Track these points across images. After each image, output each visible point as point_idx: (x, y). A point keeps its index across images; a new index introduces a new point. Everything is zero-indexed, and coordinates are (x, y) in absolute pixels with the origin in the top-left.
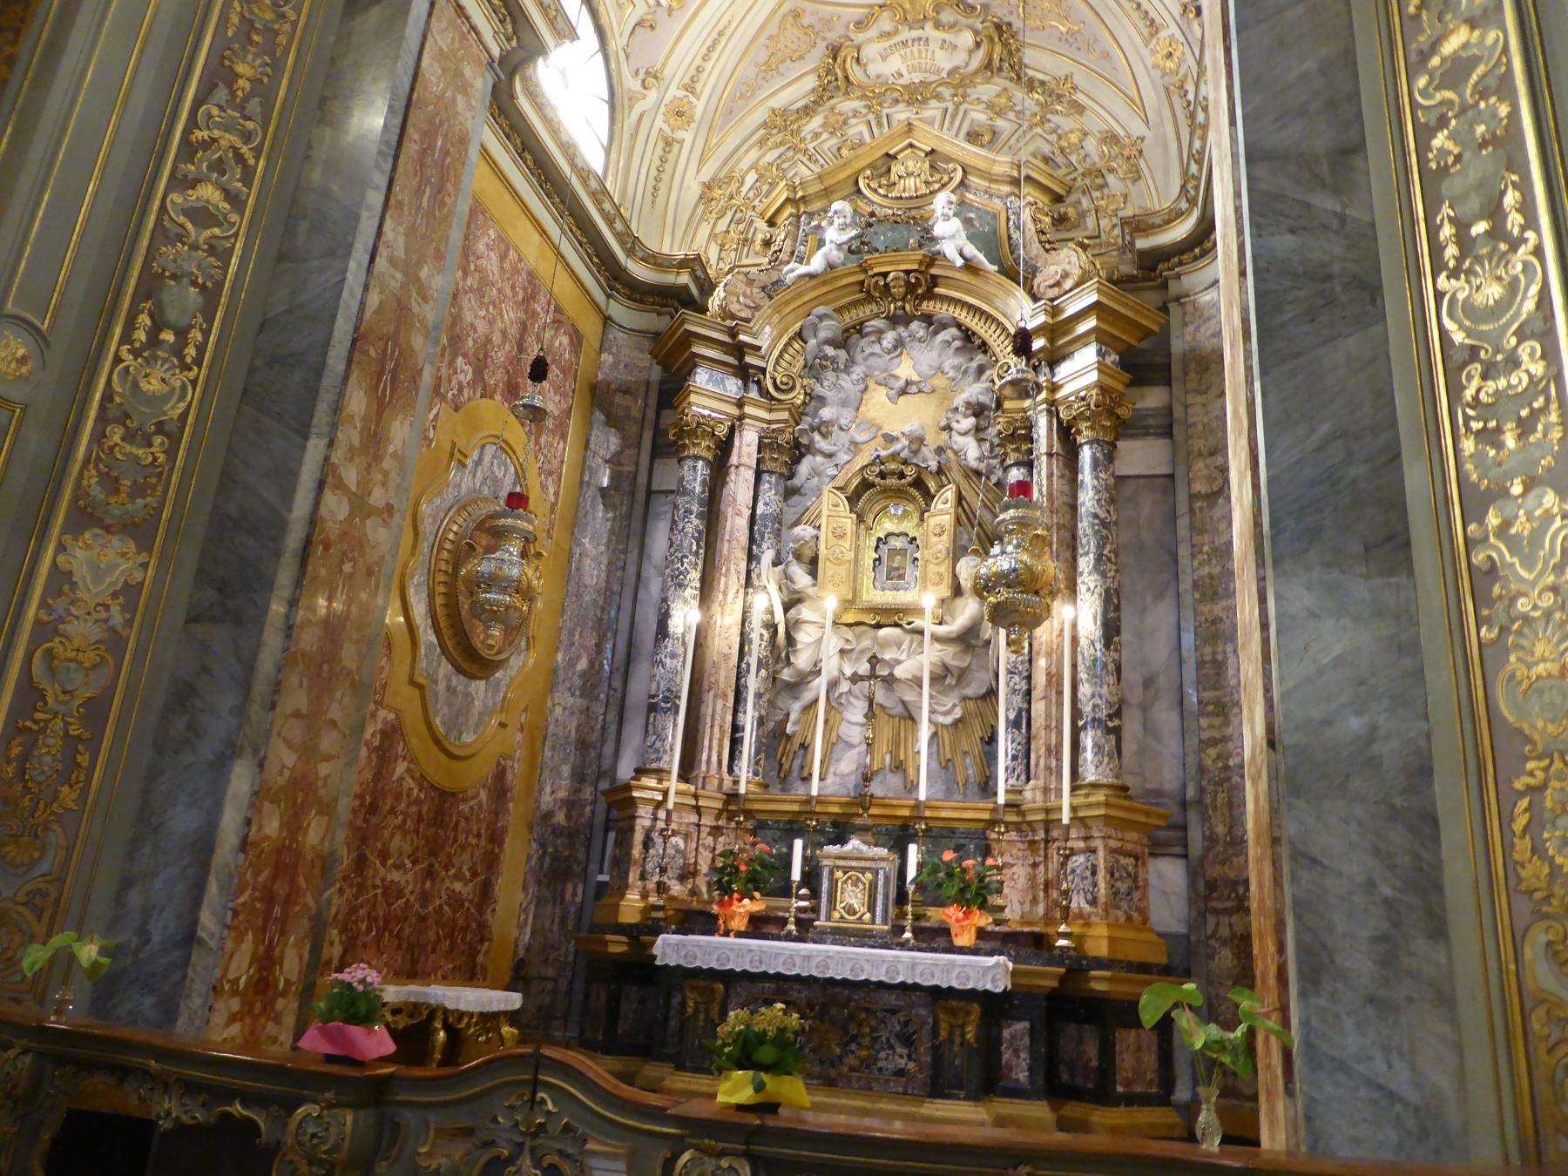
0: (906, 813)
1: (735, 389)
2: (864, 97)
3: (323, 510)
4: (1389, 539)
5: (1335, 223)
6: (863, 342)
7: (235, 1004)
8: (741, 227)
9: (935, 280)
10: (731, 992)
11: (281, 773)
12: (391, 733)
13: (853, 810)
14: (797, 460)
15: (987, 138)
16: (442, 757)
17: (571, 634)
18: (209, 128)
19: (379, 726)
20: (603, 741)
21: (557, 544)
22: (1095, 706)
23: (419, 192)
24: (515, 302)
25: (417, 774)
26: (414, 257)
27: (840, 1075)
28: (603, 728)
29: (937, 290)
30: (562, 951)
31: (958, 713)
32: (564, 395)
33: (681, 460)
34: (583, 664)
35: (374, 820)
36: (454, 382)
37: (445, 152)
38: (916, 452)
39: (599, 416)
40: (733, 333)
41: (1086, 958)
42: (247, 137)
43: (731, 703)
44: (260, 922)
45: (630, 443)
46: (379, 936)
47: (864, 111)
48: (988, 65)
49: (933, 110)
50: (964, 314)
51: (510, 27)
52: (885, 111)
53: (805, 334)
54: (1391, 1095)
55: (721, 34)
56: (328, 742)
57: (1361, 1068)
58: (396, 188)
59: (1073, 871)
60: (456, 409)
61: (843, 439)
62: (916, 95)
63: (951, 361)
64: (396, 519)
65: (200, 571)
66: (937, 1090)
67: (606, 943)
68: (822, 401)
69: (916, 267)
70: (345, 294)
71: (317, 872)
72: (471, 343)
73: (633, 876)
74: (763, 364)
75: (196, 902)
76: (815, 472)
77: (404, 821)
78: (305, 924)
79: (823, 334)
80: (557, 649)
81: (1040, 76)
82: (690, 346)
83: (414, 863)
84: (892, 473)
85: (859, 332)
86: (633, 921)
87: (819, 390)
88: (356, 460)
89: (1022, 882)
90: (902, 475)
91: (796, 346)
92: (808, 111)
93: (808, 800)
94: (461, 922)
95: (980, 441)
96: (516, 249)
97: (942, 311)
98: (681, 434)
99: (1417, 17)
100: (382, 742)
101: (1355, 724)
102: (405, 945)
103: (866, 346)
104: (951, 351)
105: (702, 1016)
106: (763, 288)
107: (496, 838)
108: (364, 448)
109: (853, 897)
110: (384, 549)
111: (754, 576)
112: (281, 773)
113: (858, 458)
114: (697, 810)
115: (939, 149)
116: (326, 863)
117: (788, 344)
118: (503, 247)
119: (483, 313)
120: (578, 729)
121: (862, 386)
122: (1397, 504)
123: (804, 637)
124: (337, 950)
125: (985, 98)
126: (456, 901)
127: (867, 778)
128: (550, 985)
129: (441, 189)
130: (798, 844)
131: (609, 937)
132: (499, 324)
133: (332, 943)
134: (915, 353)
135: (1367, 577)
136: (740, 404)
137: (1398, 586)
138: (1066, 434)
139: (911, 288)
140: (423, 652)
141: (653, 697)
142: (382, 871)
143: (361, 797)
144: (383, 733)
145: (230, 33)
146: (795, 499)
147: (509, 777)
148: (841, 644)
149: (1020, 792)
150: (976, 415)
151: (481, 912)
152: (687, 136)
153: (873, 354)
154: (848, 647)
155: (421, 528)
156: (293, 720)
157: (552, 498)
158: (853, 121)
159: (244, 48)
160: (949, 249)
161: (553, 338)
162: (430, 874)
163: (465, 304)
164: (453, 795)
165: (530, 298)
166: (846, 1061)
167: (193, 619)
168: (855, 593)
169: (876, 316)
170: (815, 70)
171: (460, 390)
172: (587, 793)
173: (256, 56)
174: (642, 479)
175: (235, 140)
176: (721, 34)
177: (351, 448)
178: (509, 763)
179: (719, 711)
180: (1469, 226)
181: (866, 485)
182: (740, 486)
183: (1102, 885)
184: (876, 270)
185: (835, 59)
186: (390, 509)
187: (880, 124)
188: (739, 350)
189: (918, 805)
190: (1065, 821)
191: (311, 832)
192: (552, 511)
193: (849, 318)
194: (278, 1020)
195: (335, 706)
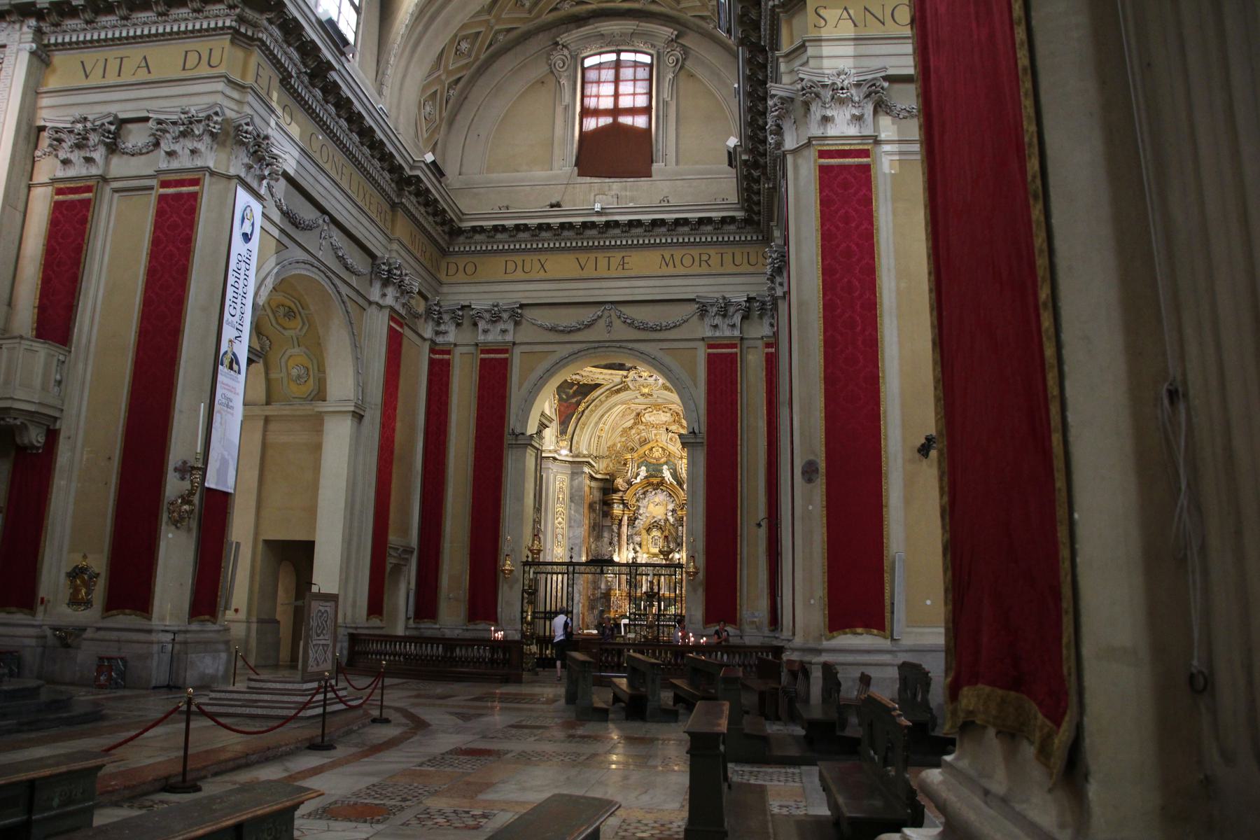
61: (644, 515)
68: (639, 507)
97: (664, 488)
103: (649, 494)
136: (623, 511)
139: (658, 484)
160: (666, 479)
182: (624, 529)
188: (623, 500)
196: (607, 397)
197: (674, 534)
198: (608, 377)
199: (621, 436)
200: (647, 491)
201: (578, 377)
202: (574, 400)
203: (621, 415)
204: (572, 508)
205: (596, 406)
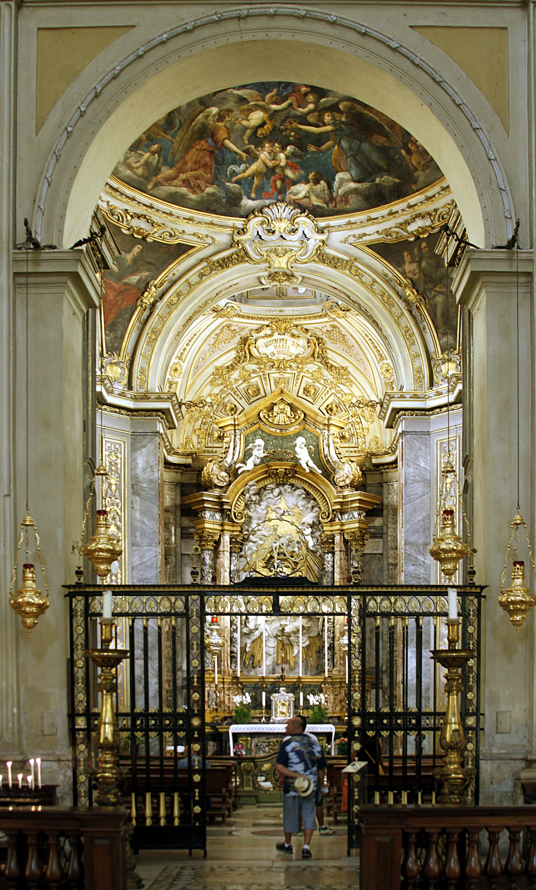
2: (257, 363)
15: (313, 391)
47: (258, 370)
48: (313, 355)
92: (231, 368)
125: (311, 371)
152: (180, 380)
158: (253, 375)
187: (265, 378)
196: (202, 275)
198: (203, 230)
201: (142, 224)
202: (134, 279)
203: (211, 341)
205: (178, 295)
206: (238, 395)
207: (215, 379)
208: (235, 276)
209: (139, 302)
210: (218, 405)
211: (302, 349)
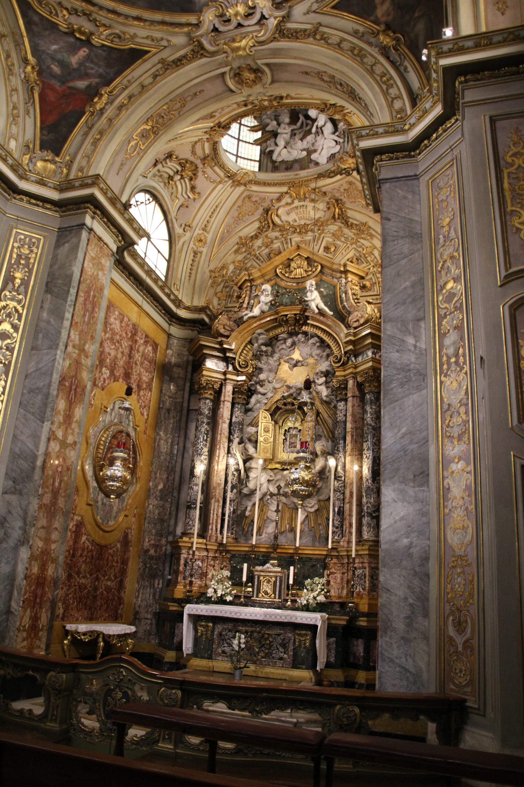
0: (291, 551)
1: (223, 367)
2: (280, 231)
3: (50, 449)
4: (422, 473)
5: (413, 348)
6: (278, 343)
7: (25, 634)
8: (228, 290)
9: (307, 318)
10: (216, 627)
11: (38, 550)
12: (80, 525)
13: (271, 550)
14: (250, 397)
15: (332, 249)
16: (101, 532)
17: (156, 474)
18: (5, 301)
19: (75, 523)
20: (170, 519)
21: (149, 436)
22: (368, 507)
23: (84, 315)
24: (128, 339)
25: (91, 540)
26: (82, 342)
27: (258, 660)
28: (170, 513)
29: (308, 321)
30: (154, 608)
31: (316, 507)
32: (150, 372)
33: (200, 399)
34: (161, 486)
35: (74, 560)
36: (102, 379)
37: (94, 296)
38: (299, 394)
39: (167, 378)
40: (221, 343)
41: (358, 612)
42: (19, 302)
43: (221, 504)
44: (32, 605)
45: (180, 389)
46: (78, 604)
47: (280, 237)
48: (334, 217)
49: (309, 237)
50: (320, 332)
51: (120, 238)
52: (289, 237)
53: (253, 341)
54: (406, 670)
55: (217, 207)
56: (55, 536)
57: (397, 661)
58: (75, 318)
59: (358, 576)
60: (103, 389)
61: (269, 387)
62: (303, 230)
63: (316, 352)
64: (78, 446)
65: (6, 474)
66: (295, 666)
67: (169, 606)
68: (260, 370)
69: (298, 312)
70: (56, 364)
71: (52, 585)
72: (108, 360)
73: (179, 579)
74: (234, 356)
75: (10, 599)
76: (258, 402)
77: (86, 559)
78: (48, 604)
79: (260, 342)
80: (150, 481)
81: (355, 222)
82: (202, 350)
83: (91, 575)
84: (289, 403)
85: (277, 339)
86: (180, 597)
87: (260, 365)
88: (62, 427)
89: (339, 580)
90: (293, 404)
91: (249, 346)
92: (256, 237)
93: (253, 546)
94: (111, 597)
95: (327, 387)
96: (127, 316)
98: (200, 389)
99: (440, 272)
100: (76, 529)
101: (405, 541)
102: (88, 608)
104: (316, 347)
105: (204, 637)
106: (235, 321)
107: (125, 562)
108: (65, 421)
109: (266, 587)
110: (73, 459)
111: (231, 449)
112: (38, 550)
113: (276, 395)
114: (207, 550)
115: (311, 257)
116: (55, 581)
117: (246, 346)
118: (121, 317)
119: (113, 347)
120: (159, 514)
121: (278, 363)
122: (425, 460)
123: (252, 475)
124: (61, 611)
125: (332, 231)
126: (108, 589)
127: (276, 537)
128: (149, 622)
129: (93, 310)
130: (245, 566)
131: (169, 604)
132: (121, 350)
133: (59, 609)
134: (300, 348)
135: (414, 487)
137: (424, 491)
138: (360, 386)
139: (297, 321)
140: (91, 490)
141: (188, 502)
142: (78, 579)
143: (69, 551)
144: (77, 525)
145: (13, 262)
146: (249, 413)
147: (130, 537)
148: (269, 478)
149: (339, 542)
150: (326, 376)
151: (119, 593)
152: (205, 250)
153: (282, 349)
154: (271, 479)
155: (90, 441)
156: (41, 530)
157: (146, 417)
158: (275, 241)
159: (18, 267)
160: (313, 305)
161: (144, 349)
162: (97, 579)
163: (106, 345)
164: (106, 547)
165: (134, 334)
166: (260, 654)
167: (5, 493)
168: (274, 454)
169: (283, 333)
170: (259, 220)
171: (104, 381)
172: (163, 541)
173: (22, 269)
174: (185, 405)
175: (15, 304)
176: (217, 207)
177: (60, 423)
178: (130, 531)
179: (216, 508)
180: (450, 358)
181: (278, 408)
182: (225, 410)
183: (367, 582)
184: (282, 314)
185: (267, 214)
186: (75, 443)
187: (287, 243)
188: (224, 351)
189: (297, 549)
190: (353, 556)
191: (49, 571)
192: (146, 422)
193: (272, 334)
194: (40, 640)
195: (57, 522)
197: (330, 421)
199: (236, 252)
200: (276, 338)
202: (81, 84)
204: (47, 306)
205: (130, 97)
206: (260, 260)
207: (239, 249)
208: (194, 75)
209: (87, 108)
210: (241, 270)
211: (322, 213)
